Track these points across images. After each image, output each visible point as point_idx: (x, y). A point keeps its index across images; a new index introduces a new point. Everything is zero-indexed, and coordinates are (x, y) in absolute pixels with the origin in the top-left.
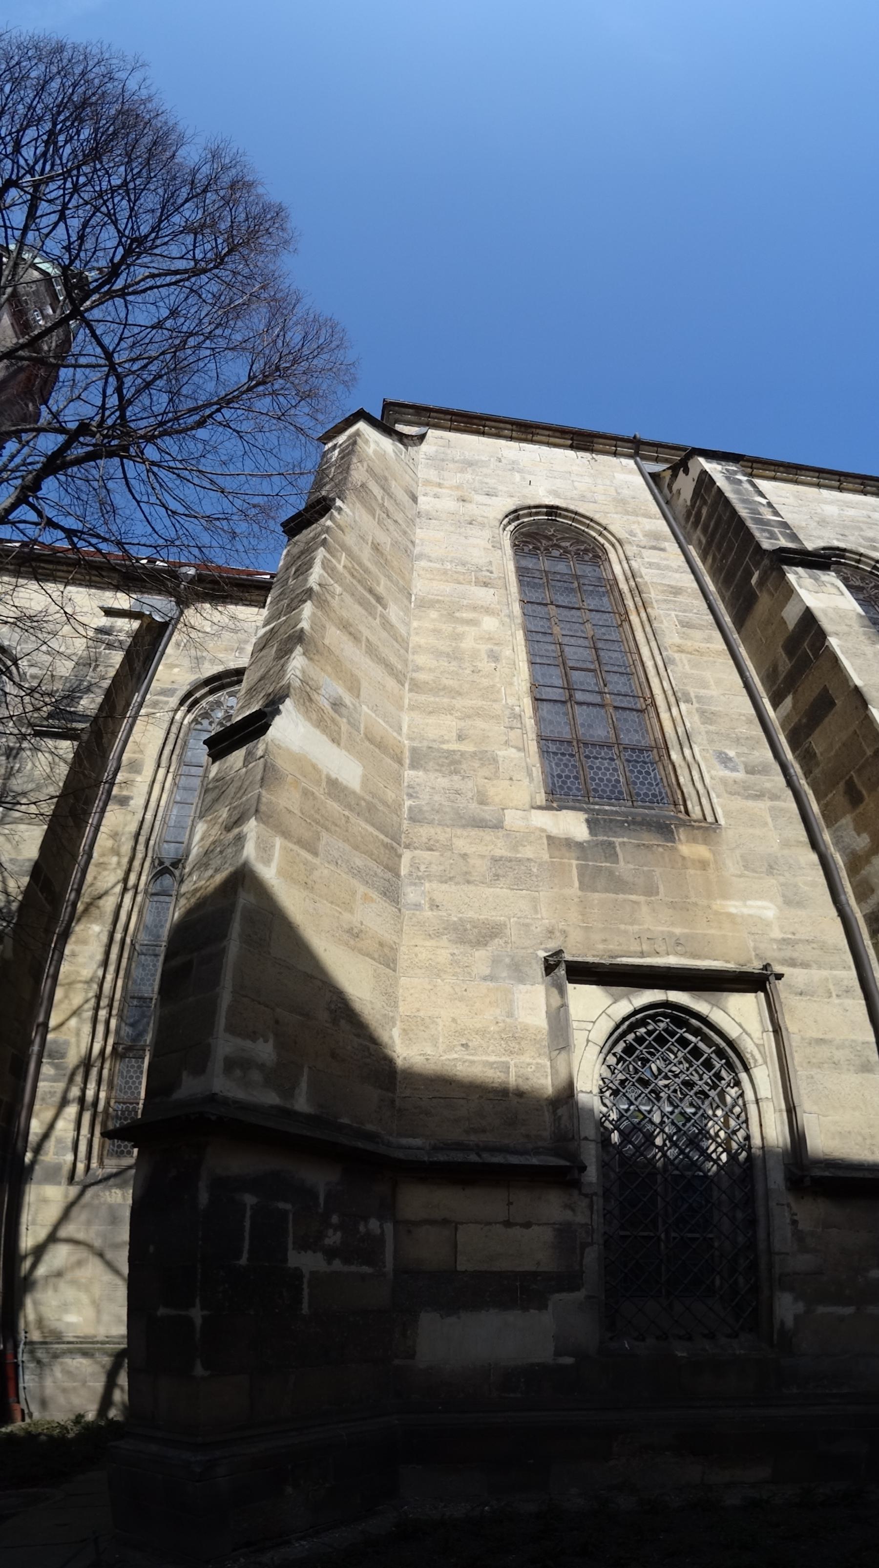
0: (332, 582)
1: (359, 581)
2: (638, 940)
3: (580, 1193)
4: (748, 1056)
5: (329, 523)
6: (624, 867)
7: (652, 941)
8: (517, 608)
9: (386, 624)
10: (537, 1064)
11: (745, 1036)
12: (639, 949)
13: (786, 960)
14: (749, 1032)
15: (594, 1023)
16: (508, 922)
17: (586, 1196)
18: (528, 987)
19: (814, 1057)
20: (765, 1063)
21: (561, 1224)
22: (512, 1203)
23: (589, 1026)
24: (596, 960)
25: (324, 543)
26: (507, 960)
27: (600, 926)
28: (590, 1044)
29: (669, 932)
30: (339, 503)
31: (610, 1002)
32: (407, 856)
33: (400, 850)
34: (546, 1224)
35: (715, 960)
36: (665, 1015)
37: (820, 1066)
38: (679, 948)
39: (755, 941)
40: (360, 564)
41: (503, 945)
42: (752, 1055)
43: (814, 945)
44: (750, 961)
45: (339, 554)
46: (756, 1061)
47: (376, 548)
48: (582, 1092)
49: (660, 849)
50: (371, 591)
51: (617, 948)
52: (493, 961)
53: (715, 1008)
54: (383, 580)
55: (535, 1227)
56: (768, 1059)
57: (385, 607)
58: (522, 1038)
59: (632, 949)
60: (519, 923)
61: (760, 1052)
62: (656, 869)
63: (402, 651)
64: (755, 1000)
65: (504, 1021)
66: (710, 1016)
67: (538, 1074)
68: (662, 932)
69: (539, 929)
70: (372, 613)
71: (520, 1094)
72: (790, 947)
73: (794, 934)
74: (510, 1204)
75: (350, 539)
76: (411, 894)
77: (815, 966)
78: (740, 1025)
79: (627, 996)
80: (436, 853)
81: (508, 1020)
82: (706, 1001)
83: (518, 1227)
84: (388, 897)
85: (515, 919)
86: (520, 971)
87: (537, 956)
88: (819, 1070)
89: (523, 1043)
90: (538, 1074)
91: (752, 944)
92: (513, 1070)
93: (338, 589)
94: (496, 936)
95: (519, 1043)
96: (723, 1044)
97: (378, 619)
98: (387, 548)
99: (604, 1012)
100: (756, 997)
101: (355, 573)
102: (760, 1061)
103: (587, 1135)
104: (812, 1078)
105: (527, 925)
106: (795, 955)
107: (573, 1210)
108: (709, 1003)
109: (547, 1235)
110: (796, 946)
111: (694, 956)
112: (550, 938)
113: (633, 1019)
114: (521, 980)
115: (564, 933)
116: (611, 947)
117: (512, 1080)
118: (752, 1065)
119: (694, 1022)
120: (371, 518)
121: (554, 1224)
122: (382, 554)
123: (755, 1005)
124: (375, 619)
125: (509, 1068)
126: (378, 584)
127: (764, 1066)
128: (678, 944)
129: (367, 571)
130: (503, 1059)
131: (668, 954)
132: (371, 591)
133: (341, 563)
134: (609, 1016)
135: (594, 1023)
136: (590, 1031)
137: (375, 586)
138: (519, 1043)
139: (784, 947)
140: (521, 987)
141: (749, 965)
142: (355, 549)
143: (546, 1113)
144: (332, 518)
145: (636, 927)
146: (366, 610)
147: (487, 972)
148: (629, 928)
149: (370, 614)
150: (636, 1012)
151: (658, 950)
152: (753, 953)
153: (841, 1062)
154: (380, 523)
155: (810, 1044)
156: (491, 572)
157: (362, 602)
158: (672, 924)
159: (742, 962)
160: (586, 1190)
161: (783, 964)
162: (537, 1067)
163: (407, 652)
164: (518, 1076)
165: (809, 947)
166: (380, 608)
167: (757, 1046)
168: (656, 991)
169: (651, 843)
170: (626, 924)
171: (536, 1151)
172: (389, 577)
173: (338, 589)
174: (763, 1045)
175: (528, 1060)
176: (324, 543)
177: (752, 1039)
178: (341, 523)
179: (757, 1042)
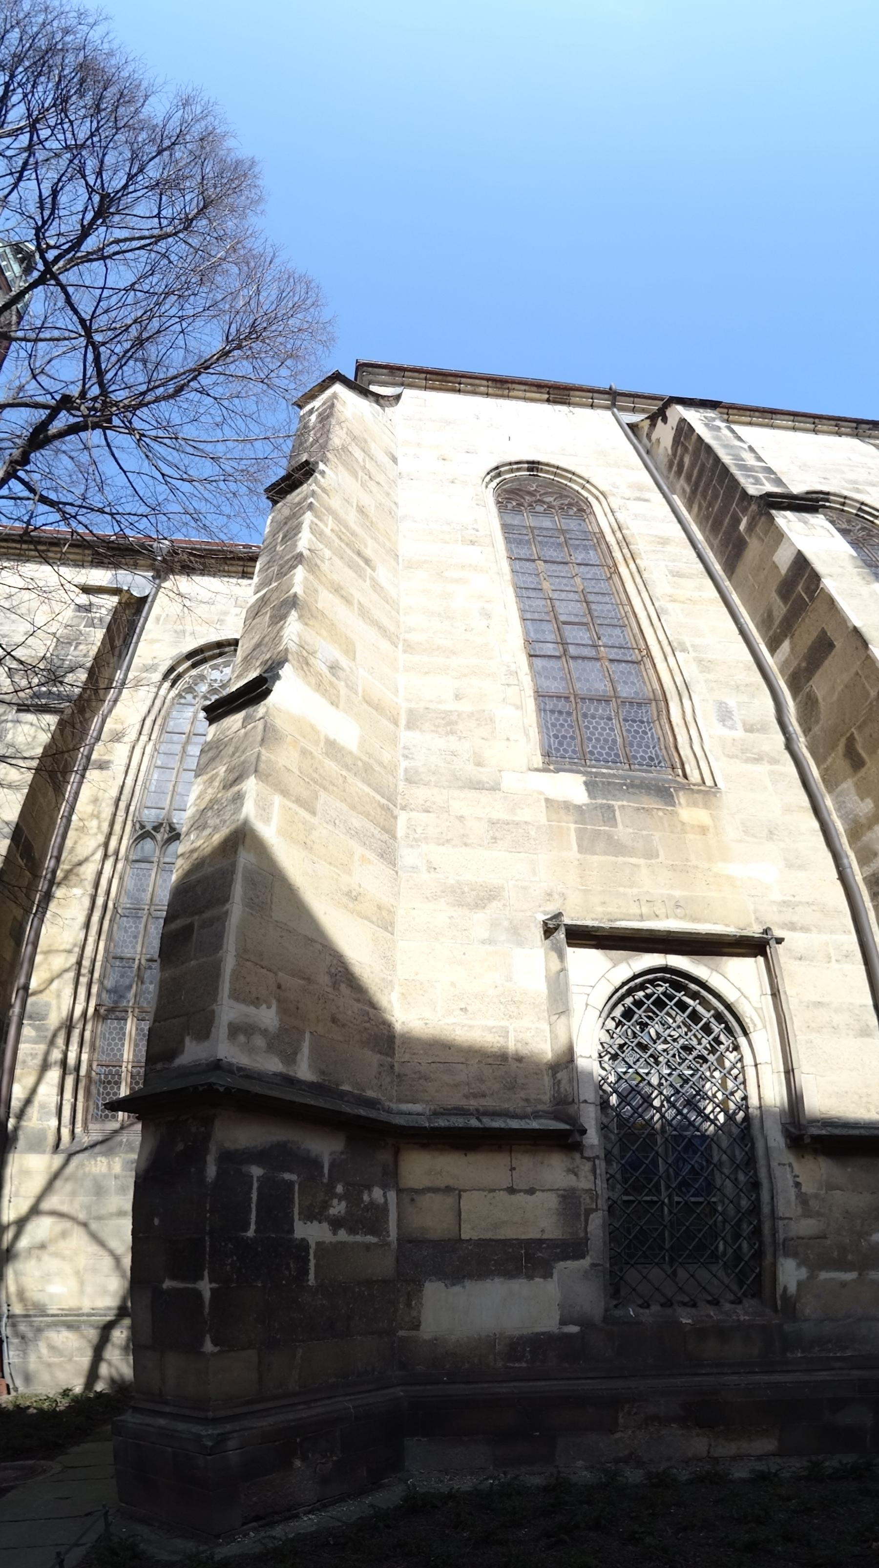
0: (321, 546)
1: (347, 544)
2: (637, 903)
3: (583, 1157)
5: (314, 487)
6: (623, 831)
7: (652, 904)
8: (505, 566)
9: (376, 586)
11: (743, 1000)
12: (638, 912)
13: (786, 924)
15: (593, 987)
17: (588, 1159)
21: (564, 1190)
22: (514, 1169)
23: (588, 990)
24: (596, 924)
25: (310, 506)
30: (321, 466)
32: (403, 818)
33: (396, 811)
34: (549, 1190)
35: (714, 924)
36: (664, 980)
38: (679, 911)
40: (347, 527)
43: (815, 908)
44: (750, 925)
45: (325, 518)
47: (361, 510)
48: (581, 1056)
49: (660, 813)
50: (359, 554)
51: (616, 910)
53: (714, 973)
54: (370, 542)
55: (538, 1193)
57: (374, 570)
58: (521, 1002)
62: (655, 833)
63: (393, 612)
64: (754, 965)
70: (360, 574)
71: (519, 1059)
72: (790, 910)
73: (794, 896)
74: (513, 1169)
75: (335, 502)
76: (407, 856)
78: (739, 990)
79: (626, 960)
80: (432, 815)
82: (706, 965)
83: (522, 1194)
84: (385, 860)
93: (327, 553)
96: (721, 1008)
97: (368, 581)
98: (372, 511)
100: (756, 962)
101: (343, 537)
103: (587, 1098)
106: (795, 919)
107: (576, 1175)
108: (709, 967)
109: (551, 1201)
111: (694, 920)
113: (632, 984)
116: (610, 909)
117: (512, 1045)
119: (693, 986)
120: (354, 480)
121: (558, 1190)
122: (367, 516)
124: (365, 581)
125: (508, 1032)
126: (366, 547)
128: (678, 906)
129: (353, 534)
130: (503, 1023)
131: (667, 917)
132: (359, 554)
133: (328, 526)
135: (593, 987)
137: (362, 548)
139: (784, 909)
141: (749, 929)
142: (341, 513)
144: (316, 482)
145: (635, 890)
146: (356, 572)
148: (629, 891)
149: (360, 576)
151: (657, 913)
154: (363, 485)
155: (808, 1007)
156: (477, 531)
157: (351, 565)
159: (741, 926)
160: (588, 1153)
163: (398, 613)
166: (369, 571)
167: (756, 1009)
168: (656, 955)
169: (651, 806)
171: (536, 1115)
172: (375, 539)
173: (327, 553)
174: (762, 1008)
176: (310, 506)
178: (325, 485)
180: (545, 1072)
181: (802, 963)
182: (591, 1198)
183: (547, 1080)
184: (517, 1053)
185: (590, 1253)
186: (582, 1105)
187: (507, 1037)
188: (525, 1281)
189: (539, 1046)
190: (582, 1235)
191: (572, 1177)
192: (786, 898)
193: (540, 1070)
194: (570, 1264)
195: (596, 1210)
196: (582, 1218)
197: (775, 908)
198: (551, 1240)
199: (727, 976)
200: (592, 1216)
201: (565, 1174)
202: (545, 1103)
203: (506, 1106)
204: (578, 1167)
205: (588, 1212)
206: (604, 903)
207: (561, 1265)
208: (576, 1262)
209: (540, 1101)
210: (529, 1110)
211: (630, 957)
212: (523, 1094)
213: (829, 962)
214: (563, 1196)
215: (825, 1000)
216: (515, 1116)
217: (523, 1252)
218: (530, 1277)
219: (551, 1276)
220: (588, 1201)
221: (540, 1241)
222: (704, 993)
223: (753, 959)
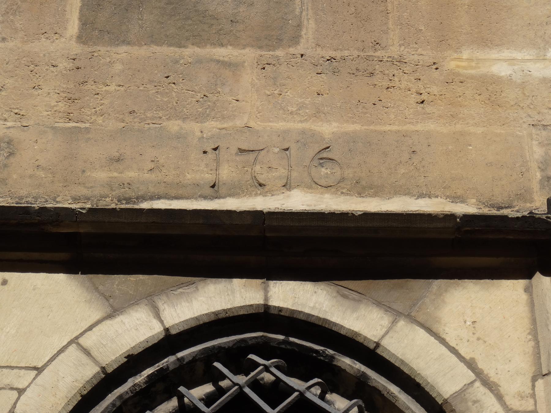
2: (211, 155)
7: (251, 157)
11: (479, 390)
12: (209, 177)
14: (493, 377)
15: (39, 370)
27: (112, 125)
29: (303, 132)
31: (96, 316)
35: (421, 196)
53: (402, 323)
64: (524, 297)
66: (385, 343)
78: (471, 364)
82: (379, 304)
99: (74, 341)
100: (528, 290)
108: (388, 309)
113: (169, 361)
116: (131, 175)
123: (522, 309)
134: (87, 352)
135: (39, 370)
136: (21, 392)
148: (194, 127)
152: (539, 175)
168: (237, 282)
170: (184, 119)
177: (500, 398)
199: (435, 328)
206: (118, 160)
211: (163, 291)
223: (521, 283)
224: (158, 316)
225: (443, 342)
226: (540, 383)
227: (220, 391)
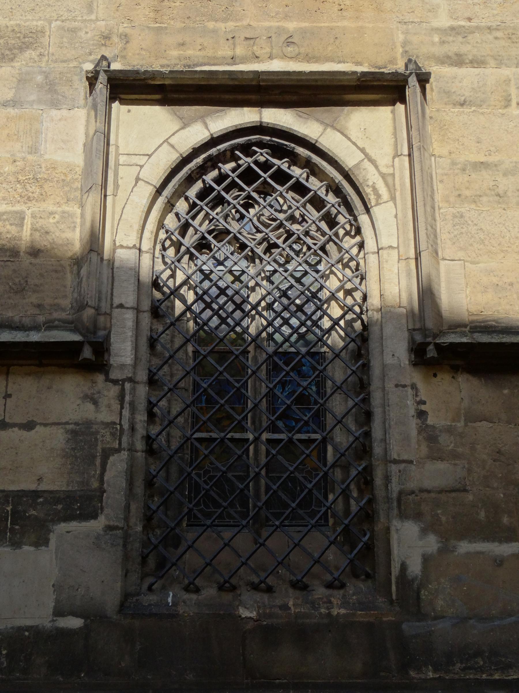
2: (231, 41)
3: (108, 379)
4: (369, 190)
7: (252, 42)
10: (64, 212)
11: (367, 164)
12: (230, 53)
13: (448, 57)
14: (374, 157)
15: (150, 156)
16: (47, 29)
17: (115, 382)
18: (64, 112)
19: (467, 188)
20: (393, 198)
21: (76, 424)
22: (10, 396)
23: (142, 160)
26: (39, 78)
27: (179, 25)
28: (140, 182)
29: (278, 28)
31: (176, 128)
35: (339, 62)
36: (261, 145)
37: (475, 200)
38: (290, 49)
39: (406, 33)
41: (37, 59)
42: (375, 189)
43: (499, 34)
44: (393, 61)
46: (378, 196)
48: (122, 247)
52: (19, 81)
53: (329, 130)
55: (38, 428)
56: (398, 194)
58: (46, 180)
59: (220, 53)
60: (63, 28)
61: (387, 184)
64: (390, 116)
65: (24, 159)
66: (320, 140)
67: (62, 226)
68: (269, 29)
69: (89, 35)
72: (460, 39)
73: (470, 19)
74: (8, 396)
77: (492, 63)
78: (363, 150)
79: (202, 118)
81: (30, 157)
82: (318, 120)
83: (16, 429)
85: (59, 23)
86: (56, 92)
87: (82, 70)
88: (473, 206)
89: (46, 186)
90: (62, 226)
91: (401, 37)
92: (28, 222)
94: (27, 47)
95: (41, 187)
96: (338, 177)
99: (166, 141)
100: (393, 112)
102: (385, 194)
103: (123, 301)
104: (462, 216)
105: (74, 31)
106: (464, 49)
107: (95, 403)
108: (322, 123)
110: (470, 37)
111: (309, 58)
112: (105, 45)
113: (213, 151)
114: (55, 104)
115: (126, 38)
116: (190, 52)
118: (373, 203)
119: (301, 151)
121: (67, 423)
123: (389, 122)
125: (24, 218)
127: (391, 204)
128: (289, 43)
130: (18, 208)
134: (173, 146)
135: (150, 156)
136: (141, 167)
138: (41, 187)
139: (451, 39)
140: (54, 113)
143: (69, 276)
145: (231, 25)
147: (10, 95)
148: (221, 26)
150: (213, 142)
151: (257, 54)
152: (401, 50)
153: (509, 194)
155: (464, 170)
158: (286, 17)
160: (115, 375)
161: (443, 63)
162: (62, 217)
164: (34, 229)
165: (491, 37)
167: (383, 176)
168: (246, 109)
170: (216, 21)
171: (50, 325)
174: (393, 175)
175: (51, 208)
177: (376, 167)
179: (384, 170)
180: (68, 268)
181: (466, 110)
182: (113, 434)
183: (69, 279)
184: (32, 247)
185: (106, 511)
186: (117, 310)
187: (21, 225)
188: (8, 549)
189: (64, 235)
190: (95, 485)
191: (90, 407)
192: (455, 23)
193: (61, 266)
194: (74, 525)
195: (118, 450)
196: (98, 461)
197: (436, 39)
198: (51, 492)
199: (347, 132)
200: (112, 459)
201: (79, 402)
202: (63, 310)
203: (10, 314)
204: (99, 392)
205: (107, 454)
206: (183, 44)
207: (62, 527)
208: (84, 524)
209: (58, 307)
210: (41, 319)
211: (208, 114)
212: (34, 299)
213: (506, 107)
214: (74, 433)
215: (491, 159)
216: (21, 328)
217: (9, 508)
218: (16, 545)
219: (46, 542)
220: (108, 438)
221: (35, 494)
222: (316, 159)
223: (389, 108)
224: (207, 128)
225: (349, 139)
226: (397, 160)
227: (239, 166)
